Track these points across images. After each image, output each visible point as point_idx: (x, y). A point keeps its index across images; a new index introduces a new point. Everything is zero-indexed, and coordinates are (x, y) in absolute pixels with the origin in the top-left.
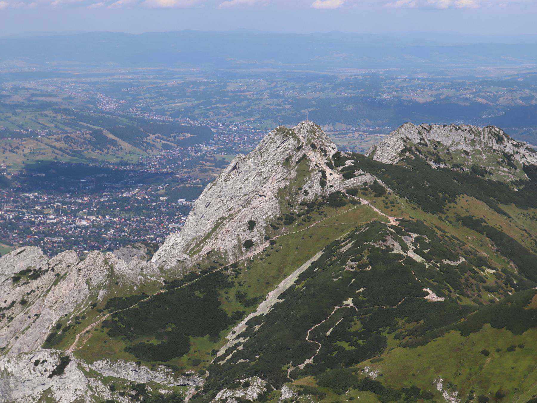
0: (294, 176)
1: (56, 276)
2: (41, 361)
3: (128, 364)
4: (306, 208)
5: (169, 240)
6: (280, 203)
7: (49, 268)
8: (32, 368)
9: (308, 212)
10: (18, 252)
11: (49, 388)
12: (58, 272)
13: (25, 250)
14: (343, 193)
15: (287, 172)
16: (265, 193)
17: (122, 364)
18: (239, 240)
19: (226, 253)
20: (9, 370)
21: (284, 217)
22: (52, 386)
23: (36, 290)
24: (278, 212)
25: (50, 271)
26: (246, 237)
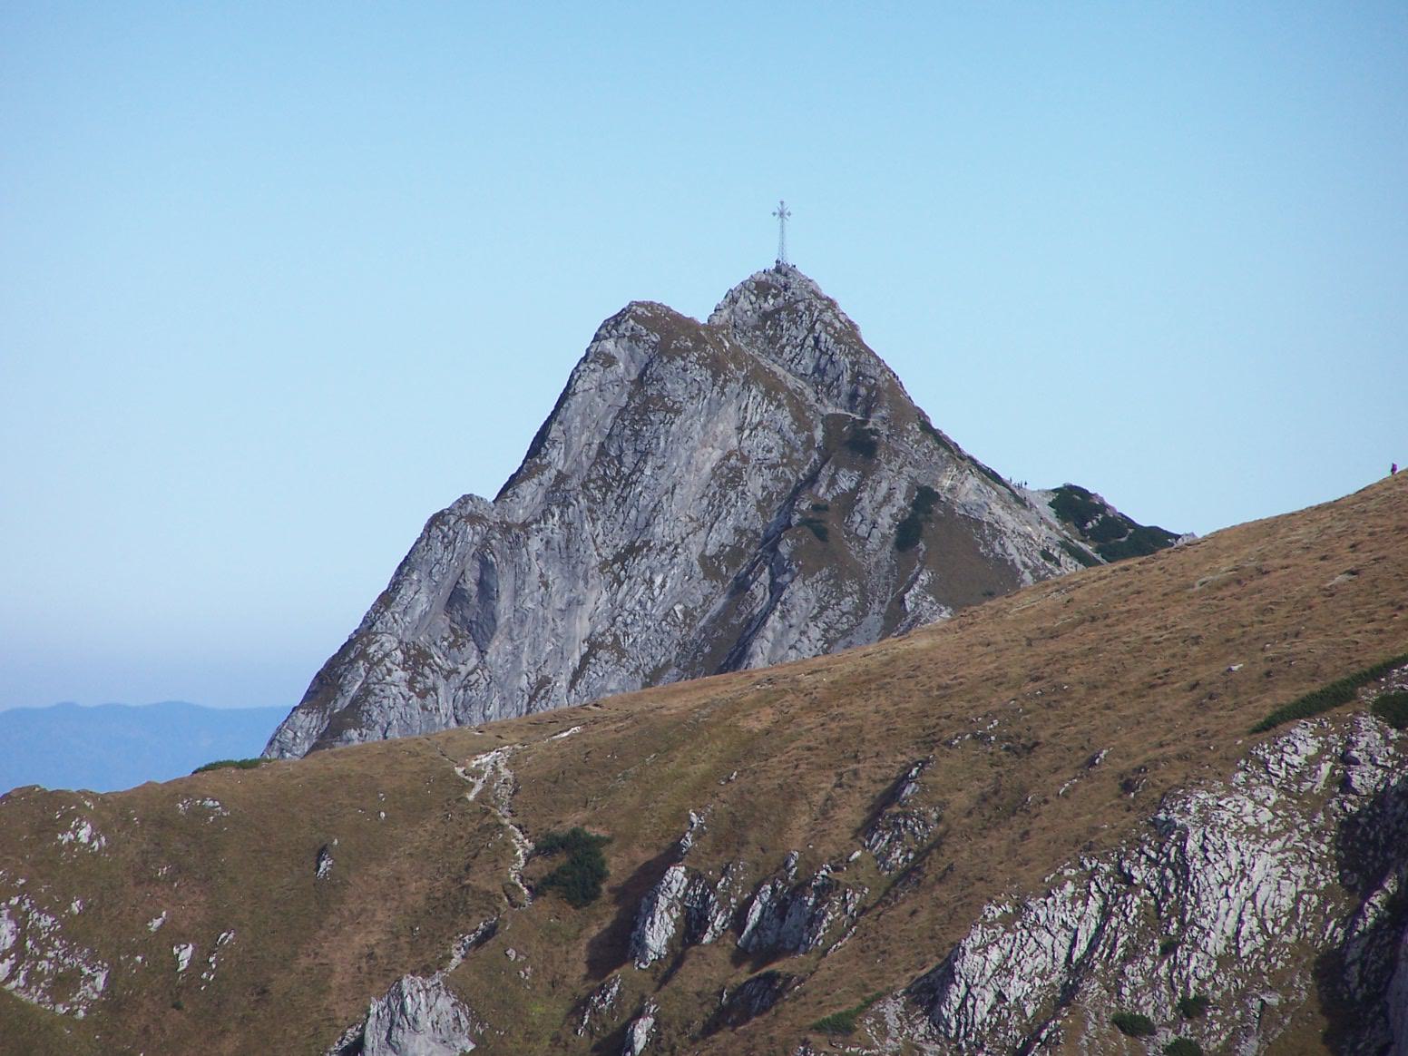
15: (861, 611)
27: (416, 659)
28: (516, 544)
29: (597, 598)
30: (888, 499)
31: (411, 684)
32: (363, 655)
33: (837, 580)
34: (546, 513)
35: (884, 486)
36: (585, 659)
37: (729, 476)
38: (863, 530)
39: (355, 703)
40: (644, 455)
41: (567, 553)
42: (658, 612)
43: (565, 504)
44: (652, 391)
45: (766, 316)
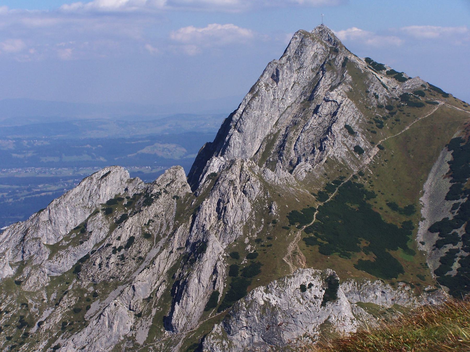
0: (351, 80)
1: (174, 198)
2: (307, 286)
3: (375, 284)
4: (387, 111)
5: (213, 166)
6: (357, 106)
7: (161, 190)
8: (299, 296)
9: (392, 114)
10: (102, 175)
11: (326, 321)
12: (175, 194)
13: (110, 172)
14: (412, 95)
15: (337, 77)
16: (335, 97)
17: (370, 284)
18: (345, 145)
19: (343, 161)
20: (273, 303)
21: (374, 122)
22: (329, 317)
23: (155, 219)
24: (363, 116)
25: (163, 194)
26: (352, 143)
27: (267, 85)
28: (282, 67)
29: (295, 75)
30: (340, 59)
31: (266, 89)
32: (258, 85)
33: (333, 72)
34: (287, 62)
35: (340, 57)
36: (293, 85)
37: (315, 56)
38: (337, 64)
39: (257, 92)
40: (302, 53)
41: (290, 69)
42: (305, 77)
43: (290, 60)
44: (303, 43)
45: (320, 32)
